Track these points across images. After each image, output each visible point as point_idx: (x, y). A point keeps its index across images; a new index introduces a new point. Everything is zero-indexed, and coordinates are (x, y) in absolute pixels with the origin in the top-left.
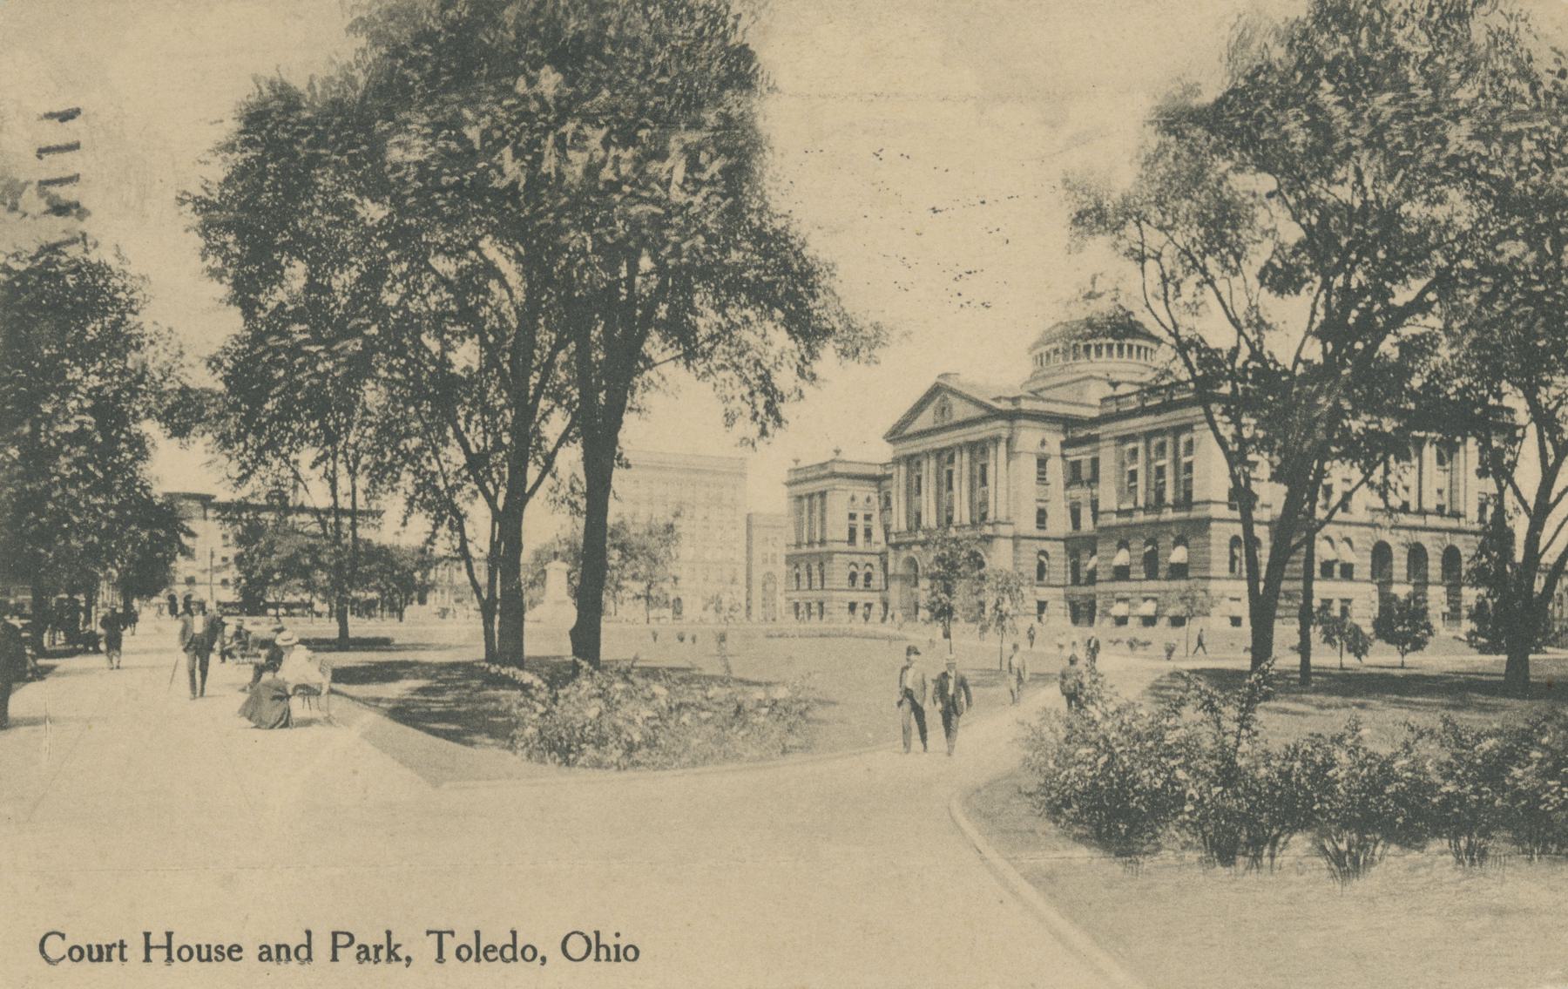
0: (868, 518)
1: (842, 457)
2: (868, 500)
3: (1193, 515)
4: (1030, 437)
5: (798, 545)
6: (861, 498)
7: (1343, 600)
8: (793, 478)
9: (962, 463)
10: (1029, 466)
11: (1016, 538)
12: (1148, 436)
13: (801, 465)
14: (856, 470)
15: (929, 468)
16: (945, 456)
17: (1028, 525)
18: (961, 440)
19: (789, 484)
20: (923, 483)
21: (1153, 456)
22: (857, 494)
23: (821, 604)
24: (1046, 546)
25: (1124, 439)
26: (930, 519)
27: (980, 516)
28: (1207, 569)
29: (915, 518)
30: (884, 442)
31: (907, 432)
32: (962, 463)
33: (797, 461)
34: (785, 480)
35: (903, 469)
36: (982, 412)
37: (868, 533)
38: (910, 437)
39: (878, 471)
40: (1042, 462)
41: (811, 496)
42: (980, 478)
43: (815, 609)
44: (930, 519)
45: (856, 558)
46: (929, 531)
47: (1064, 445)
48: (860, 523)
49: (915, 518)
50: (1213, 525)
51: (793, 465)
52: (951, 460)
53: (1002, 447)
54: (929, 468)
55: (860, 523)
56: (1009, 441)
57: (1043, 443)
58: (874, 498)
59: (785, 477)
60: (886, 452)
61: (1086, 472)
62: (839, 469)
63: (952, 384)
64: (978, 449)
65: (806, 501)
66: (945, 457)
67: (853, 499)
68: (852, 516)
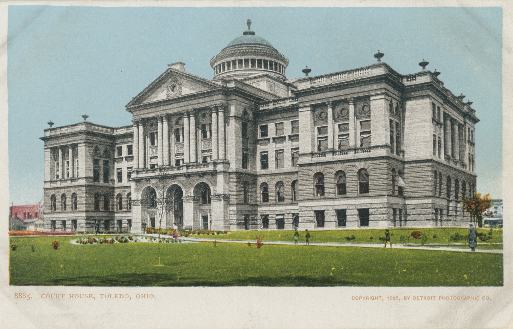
8: (48, 134)
12: (335, 104)
13: (53, 126)
15: (162, 128)
18: (189, 108)
21: (336, 117)
31: (146, 102)
33: (51, 124)
35: (141, 128)
36: (204, 89)
38: (146, 107)
41: (64, 148)
51: (48, 127)
54: (162, 128)
66: (174, 120)
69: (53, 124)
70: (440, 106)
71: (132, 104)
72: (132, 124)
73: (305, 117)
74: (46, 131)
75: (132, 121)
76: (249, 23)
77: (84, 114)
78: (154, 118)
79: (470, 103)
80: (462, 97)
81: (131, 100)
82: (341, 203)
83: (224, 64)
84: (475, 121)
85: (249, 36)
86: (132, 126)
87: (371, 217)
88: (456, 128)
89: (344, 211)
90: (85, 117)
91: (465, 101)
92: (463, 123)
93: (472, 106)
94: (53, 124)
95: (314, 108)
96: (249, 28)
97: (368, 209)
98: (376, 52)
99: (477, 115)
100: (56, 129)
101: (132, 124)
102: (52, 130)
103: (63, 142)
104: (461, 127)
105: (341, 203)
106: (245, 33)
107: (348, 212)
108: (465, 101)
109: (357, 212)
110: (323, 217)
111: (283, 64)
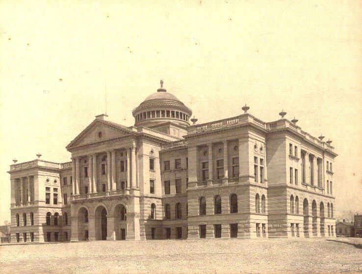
0: (55, 190)
1: (41, 158)
2: (55, 181)
3: (241, 183)
4: (147, 148)
5: (18, 204)
6: (52, 179)
7: (262, 224)
11: (142, 198)
12: (215, 145)
13: (17, 163)
14: (49, 166)
16: (102, 157)
17: (147, 191)
18: (111, 149)
19: (10, 173)
20: (89, 171)
22: (49, 178)
23: (32, 234)
24: (154, 201)
25: (200, 148)
26: (93, 188)
27: (122, 185)
28: (249, 210)
29: (85, 190)
31: (81, 144)
33: (15, 161)
34: (9, 170)
37: (55, 195)
39: (60, 167)
40: (152, 161)
41: (25, 178)
43: (29, 236)
44: (93, 188)
45: (50, 210)
46: (93, 195)
48: (52, 192)
49: (85, 190)
50: (251, 187)
51: (13, 163)
52: (104, 159)
53: (134, 153)
55: (52, 192)
56: (136, 149)
57: (152, 152)
58: (58, 180)
60: (67, 157)
61: (183, 164)
62: (40, 164)
63: (105, 119)
64: (122, 153)
65: (21, 181)
66: (101, 157)
67: (48, 180)
68: (48, 189)
69: (17, 161)
71: (71, 146)
72: (71, 161)
73: (193, 155)
74: (11, 166)
75: (71, 159)
77: (38, 154)
78: (86, 156)
80: (321, 138)
81: (70, 142)
82: (218, 219)
83: (145, 113)
84: (333, 156)
86: (71, 162)
87: (239, 230)
88: (315, 161)
89: (220, 225)
90: (39, 156)
91: (324, 140)
92: (322, 158)
93: (331, 144)
94: (17, 161)
95: (200, 148)
97: (237, 224)
98: (243, 105)
99: (334, 151)
100: (18, 165)
101: (71, 161)
102: (15, 165)
103: (24, 174)
104: (319, 160)
105: (218, 219)
107: (223, 226)
108: (324, 140)
109: (229, 226)
110: (205, 230)
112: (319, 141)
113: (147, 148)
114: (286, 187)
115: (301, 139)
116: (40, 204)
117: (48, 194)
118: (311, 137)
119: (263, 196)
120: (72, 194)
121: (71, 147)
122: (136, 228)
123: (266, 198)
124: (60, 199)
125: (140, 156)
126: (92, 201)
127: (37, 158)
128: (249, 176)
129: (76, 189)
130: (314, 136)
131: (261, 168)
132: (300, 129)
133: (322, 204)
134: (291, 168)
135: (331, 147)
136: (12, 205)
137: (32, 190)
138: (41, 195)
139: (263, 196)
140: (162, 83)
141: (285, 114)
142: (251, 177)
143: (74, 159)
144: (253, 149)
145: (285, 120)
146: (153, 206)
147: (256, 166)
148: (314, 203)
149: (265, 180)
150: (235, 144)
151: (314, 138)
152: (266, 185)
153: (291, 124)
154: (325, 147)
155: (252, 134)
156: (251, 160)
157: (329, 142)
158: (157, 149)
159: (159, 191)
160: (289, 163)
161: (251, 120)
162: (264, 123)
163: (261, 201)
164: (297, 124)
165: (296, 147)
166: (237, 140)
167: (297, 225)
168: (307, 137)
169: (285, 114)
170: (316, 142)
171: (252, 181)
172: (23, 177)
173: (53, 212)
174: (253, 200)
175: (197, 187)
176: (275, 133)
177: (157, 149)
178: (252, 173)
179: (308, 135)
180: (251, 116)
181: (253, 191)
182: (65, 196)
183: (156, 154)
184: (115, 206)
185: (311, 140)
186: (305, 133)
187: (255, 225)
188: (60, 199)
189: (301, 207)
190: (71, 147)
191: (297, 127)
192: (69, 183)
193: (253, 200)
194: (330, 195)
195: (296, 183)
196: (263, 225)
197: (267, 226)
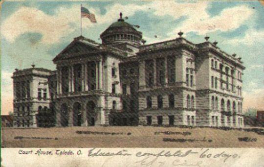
9: (84, 71)
10: (109, 70)
15: (72, 73)
24: (114, 99)
26: (72, 88)
27: (92, 87)
30: (52, 62)
32: (84, 71)
40: (113, 71)
42: (92, 74)
44: (72, 88)
45: (41, 105)
47: (120, 65)
52: (80, 69)
53: (101, 63)
55: (42, 92)
57: (114, 64)
59: (12, 75)
60: (53, 67)
62: (35, 72)
68: (39, 89)
70: (216, 60)
72: (56, 70)
76: (121, 14)
79: (240, 59)
80: (234, 55)
84: (243, 68)
85: (120, 22)
90: (33, 66)
91: (237, 57)
93: (241, 60)
96: (121, 17)
98: (179, 32)
99: (244, 65)
101: (56, 70)
106: (119, 20)
107: (163, 117)
108: (237, 57)
111: (138, 37)
112: (232, 58)
113: (110, 61)
114: (209, 90)
115: (220, 55)
116: (35, 100)
117: (40, 93)
118: (227, 55)
119: (193, 97)
120: (56, 93)
121: (55, 60)
122: (103, 118)
123: (195, 98)
124: (48, 96)
125: (106, 67)
126: (70, 98)
127: (32, 67)
128: (182, 83)
129: (59, 89)
130: (229, 54)
131: (192, 76)
132: (219, 49)
133: (234, 103)
134: (212, 77)
135: (241, 62)
136: (14, 101)
137: (29, 89)
138: (35, 94)
139: (193, 97)
140: (121, 14)
141: (208, 38)
142: (185, 83)
143: (57, 68)
144: (184, 63)
145: (209, 42)
146: (114, 102)
147: (187, 75)
148: (229, 102)
149: (194, 85)
150: (172, 60)
151: (229, 56)
152: (195, 88)
153: (213, 45)
154: (237, 62)
155: (185, 52)
156: (184, 70)
157: (240, 59)
158: (117, 62)
159: (119, 90)
160: (212, 73)
161: (184, 42)
162: (193, 45)
163: (191, 100)
164: (217, 45)
165: (216, 62)
166: (174, 56)
167: (217, 117)
168: (224, 55)
169: (208, 38)
170: (230, 58)
171: (184, 85)
172: (22, 80)
173: (43, 106)
174: (185, 99)
175: (145, 89)
176: (202, 52)
177: (117, 62)
178: (184, 79)
179: (225, 53)
180: (185, 39)
181: (185, 93)
182: (52, 95)
183: (117, 66)
184: (87, 102)
185: (228, 57)
186: (223, 52)
187: (186, 117)
188: (48, 96)
189: (219, 105)
190: (55, 60)
191: (217, 48)
192: (54, 86)
193: (185, 99)
194: (239, 96)
195: (216, 87)
196: (193, 117)
197: (195, 118)
